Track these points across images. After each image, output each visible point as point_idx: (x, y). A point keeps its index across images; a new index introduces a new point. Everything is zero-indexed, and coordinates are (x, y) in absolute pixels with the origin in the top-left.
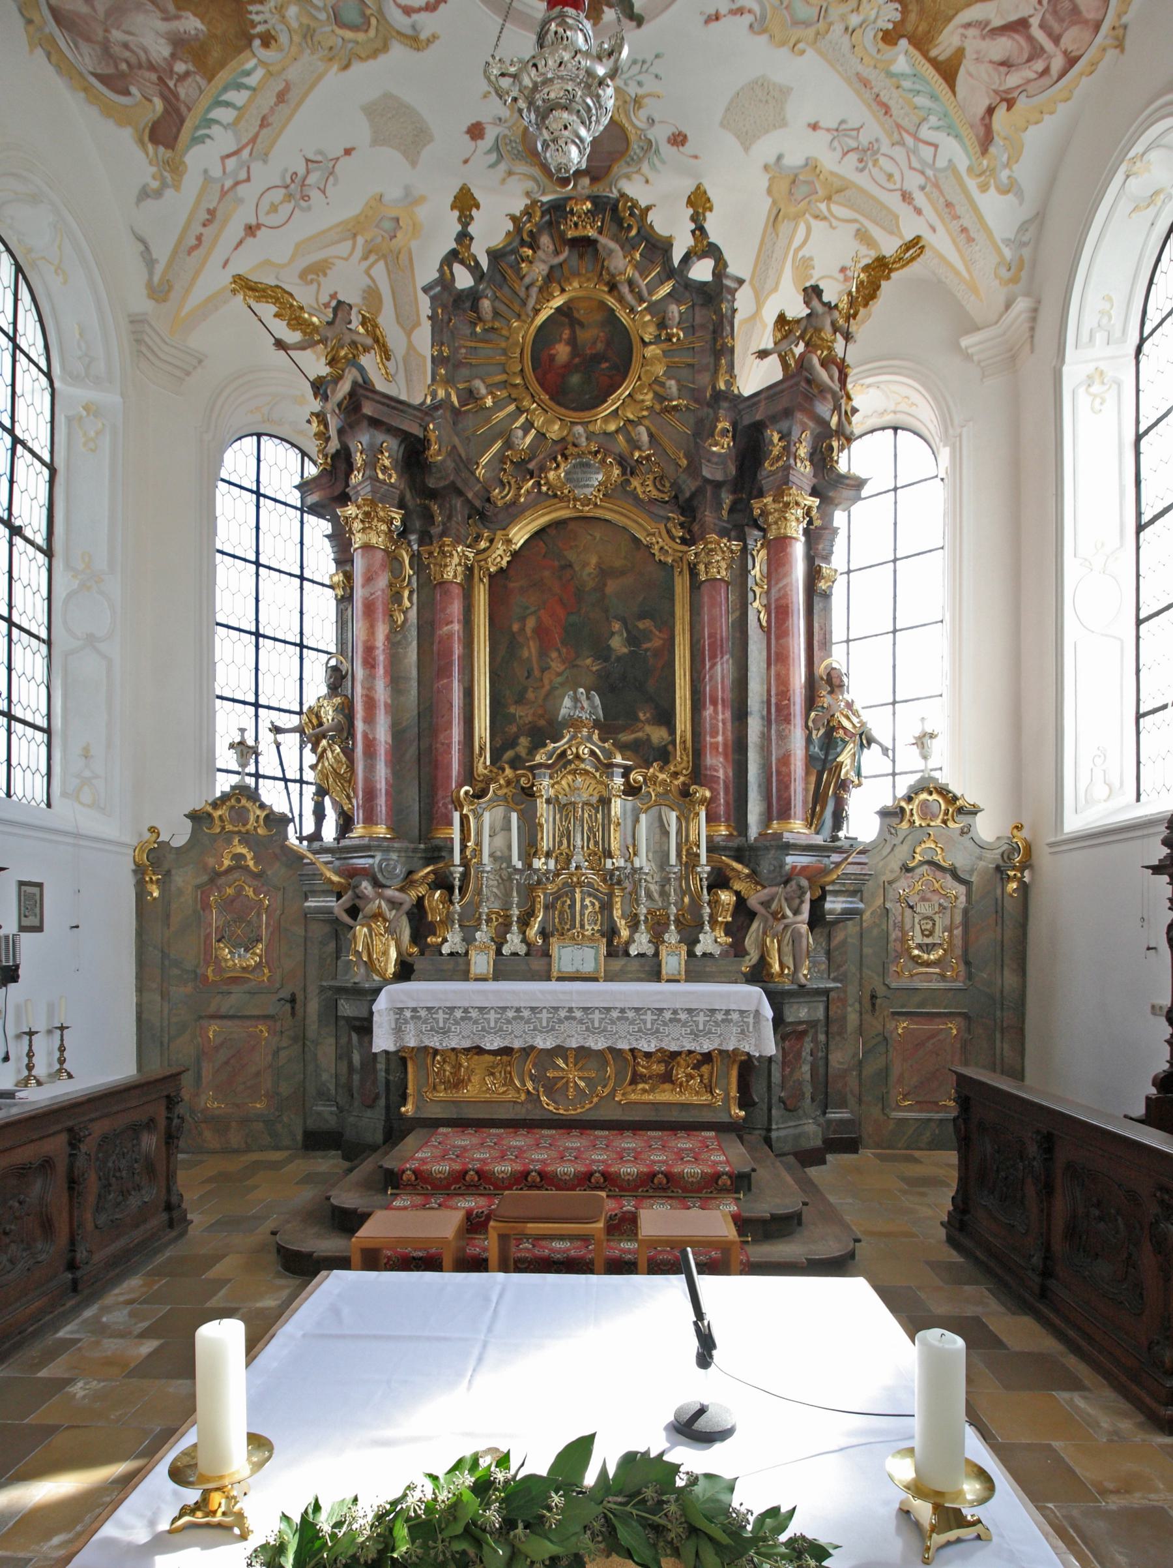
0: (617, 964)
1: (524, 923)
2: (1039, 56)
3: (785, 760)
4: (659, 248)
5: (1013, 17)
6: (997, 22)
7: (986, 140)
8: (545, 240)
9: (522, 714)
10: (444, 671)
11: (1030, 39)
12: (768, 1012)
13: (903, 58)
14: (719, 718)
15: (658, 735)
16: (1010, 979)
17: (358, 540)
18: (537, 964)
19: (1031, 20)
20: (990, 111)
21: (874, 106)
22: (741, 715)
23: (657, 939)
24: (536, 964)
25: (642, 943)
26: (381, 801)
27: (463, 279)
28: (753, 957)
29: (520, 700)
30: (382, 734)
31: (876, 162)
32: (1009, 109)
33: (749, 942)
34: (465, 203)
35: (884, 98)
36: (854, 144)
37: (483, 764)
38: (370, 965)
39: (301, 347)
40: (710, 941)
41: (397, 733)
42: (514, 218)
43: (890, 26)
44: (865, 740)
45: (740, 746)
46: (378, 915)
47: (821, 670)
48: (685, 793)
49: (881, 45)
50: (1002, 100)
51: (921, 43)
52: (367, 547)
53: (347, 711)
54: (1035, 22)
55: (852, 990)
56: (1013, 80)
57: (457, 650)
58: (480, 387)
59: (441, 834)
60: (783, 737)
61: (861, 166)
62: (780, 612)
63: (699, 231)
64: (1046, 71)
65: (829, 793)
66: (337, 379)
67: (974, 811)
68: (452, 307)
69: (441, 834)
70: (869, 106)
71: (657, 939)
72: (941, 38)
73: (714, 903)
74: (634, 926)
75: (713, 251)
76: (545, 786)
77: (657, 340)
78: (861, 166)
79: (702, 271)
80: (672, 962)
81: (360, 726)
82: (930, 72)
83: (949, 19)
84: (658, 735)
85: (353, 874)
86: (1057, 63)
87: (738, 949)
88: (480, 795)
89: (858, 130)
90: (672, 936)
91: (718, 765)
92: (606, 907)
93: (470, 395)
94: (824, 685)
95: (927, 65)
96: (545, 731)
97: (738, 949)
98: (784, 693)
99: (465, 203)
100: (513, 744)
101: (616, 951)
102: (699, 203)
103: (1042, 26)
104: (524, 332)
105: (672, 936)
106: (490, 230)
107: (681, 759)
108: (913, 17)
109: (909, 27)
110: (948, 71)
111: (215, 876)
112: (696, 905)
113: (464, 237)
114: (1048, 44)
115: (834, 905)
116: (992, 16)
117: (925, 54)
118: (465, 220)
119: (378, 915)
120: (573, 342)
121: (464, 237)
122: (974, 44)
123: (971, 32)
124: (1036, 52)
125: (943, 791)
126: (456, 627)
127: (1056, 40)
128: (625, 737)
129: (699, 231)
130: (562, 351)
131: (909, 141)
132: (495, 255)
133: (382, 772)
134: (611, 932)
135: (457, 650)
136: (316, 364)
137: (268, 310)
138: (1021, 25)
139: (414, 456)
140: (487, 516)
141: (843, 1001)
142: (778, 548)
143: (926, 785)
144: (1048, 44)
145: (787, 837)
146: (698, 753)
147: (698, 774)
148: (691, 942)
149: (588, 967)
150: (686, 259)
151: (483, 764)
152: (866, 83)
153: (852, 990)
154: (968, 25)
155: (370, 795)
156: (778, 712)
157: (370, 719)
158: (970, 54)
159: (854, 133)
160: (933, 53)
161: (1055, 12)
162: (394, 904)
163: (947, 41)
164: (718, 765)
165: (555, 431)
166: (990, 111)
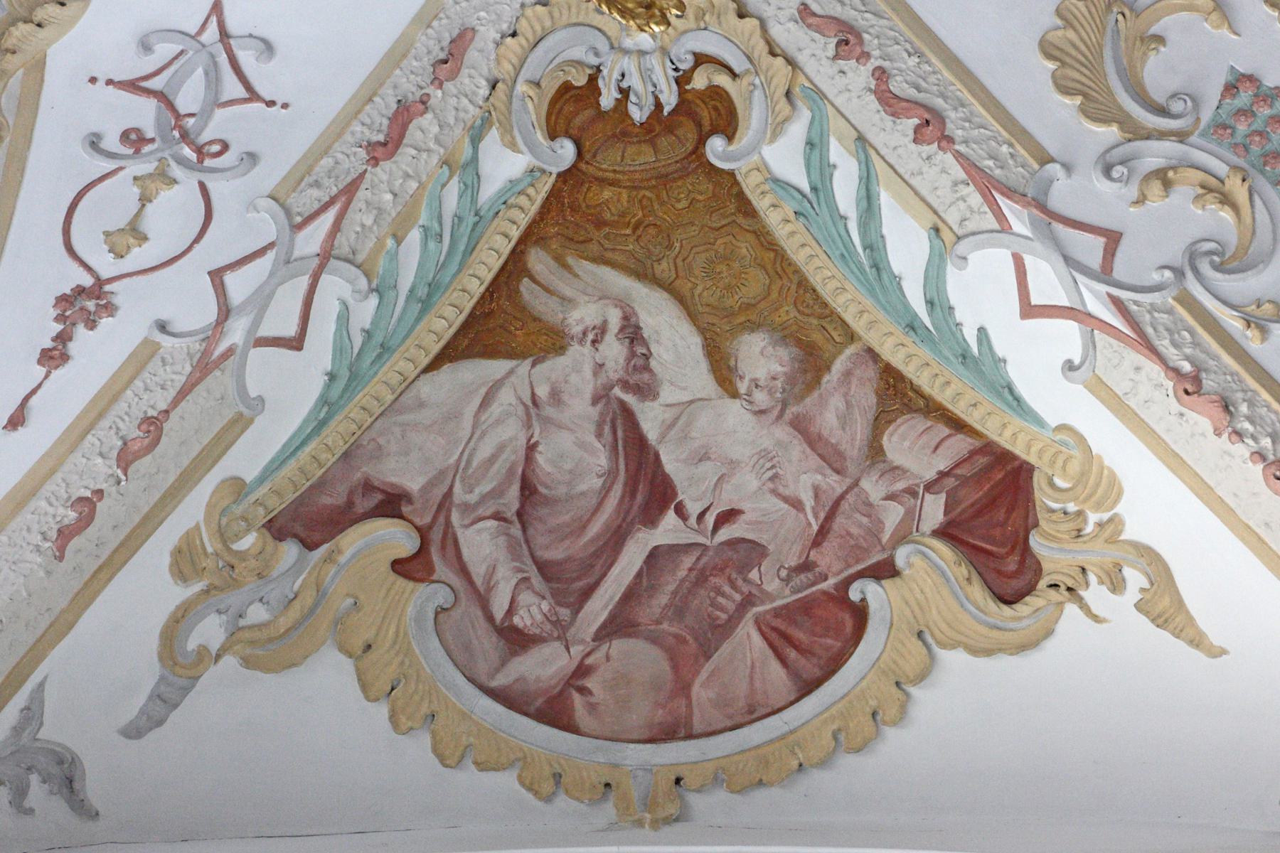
2: (559, 598)
5: (671, 463)
6: (651, 419)
7: (310, 521)
11: (615, 540)
13: (515, 164)
19: (670, 517)
20: (391, 504)
21: (386, 103)
31: (163, 177)
32: (399, 566)
35: (424, 128)
36: (189, 98)
43: (607, 100)
49: (551, 88)
50: (424, 533)
51: (566, 216)
54: (668, 530)
56: (481, 544)
61: (112, 142)
64: (516, 640)
70: (367, 96)
72: (585, 268)
78: (112, 142)
82: (489, 262)
83: (643, 274)
86: (543, 666)
89: (253, 96)
95: (506, 248)
103: (654, 556)
108: (642, 158)
109: (608, 160)
110: (496, 325)
114: (599, 608)
116: (668, 394)
117: (530, 237)
122: (576, 373)
123: (614, 351)
124: (568, 583)
127: (619, 624)
131: (311, 240)
138: (649, 489)
144: (599, 608)
152: (450, 61)
154: (633, 334)
158: (555, 366)
159: (233, 88)
160: (538, 261)
161: (701, 578)
163: (586, 295)
166: (391, 504)
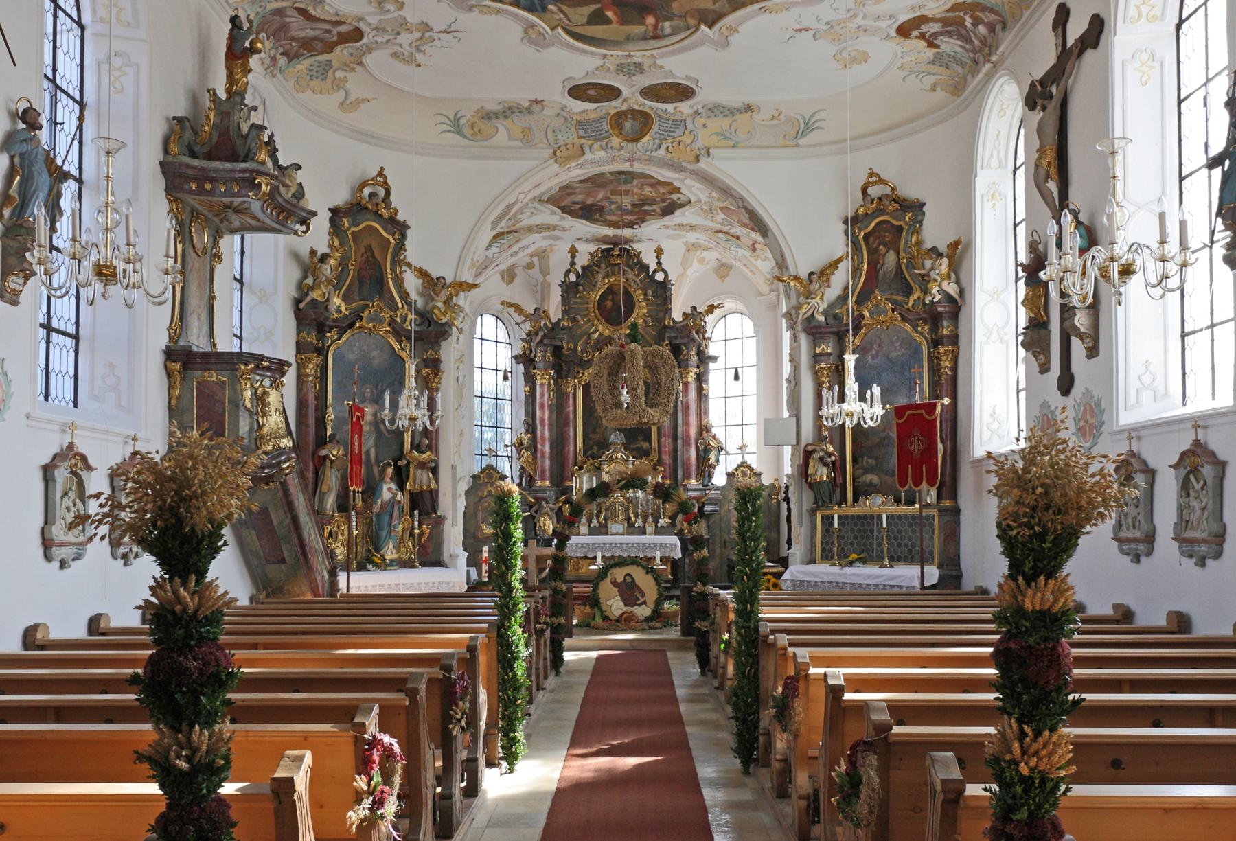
0: (631, 530)
1: (598, 516)
3: (689, 459)
4: (645, 268)
8: (603, 265)
9: (594, 437)
10: (566, 424)
12: (679, 544)
14: (667, 443)
15: (645, 445)
16: (774, 535)
17: (538, 382)
18: (603, 530)
22: (675, 438)
23: (645, 521)
24: (602, 530)
25: (639, 523)
26: (547, 473)
27: (573, 278)
28: (679, 527)
29: (594, 431)
30: (547, 449)
33: (677, 522)
34: (573, 252)
37: (580, 457)
38: (544, 531)
39: (523, 322)
40: (663, 522)
41: (551, 448)
42: (591, 255)
44: (720, 449)
45: (675, 450)
46: (547, 513)
47: (704, 423)
48: (655, 468)
52: (542, 385)
53: (534, 439)
55: (718, 540)
57: (571, 416)
58: (578, 317)
59: (568, 483)
60: (688, 451)
62: (686, 408)
63: (659, 263)
65: (705, 469)
66: (537, 334)
67: (760, 474)
68: (569, 289)
69: (568, 483)
71: (645, 521)
73: (664, 508)
74: (637, 517)
75: (663, 270)
76: (605, 467)
77: (644, 300)
79: (660, 277)
80: (649, 529)
81: (539, 446)
84: (645, 445)
85: (538, 500)
87: (673, 525)
88: (581, 468)
90: (650, 520)
91: (667, 459)
92: (627, 510)
93: (574, 320)
94: (704, 429)
96: (604, 445)
97: (673, 525)
98: (688, 436)
99: (573, 252)
100: (591, 448)
101: (630, 525)
102: (659, 252)
104: (596, 296)
105: (650, 520)
106: (582, 260)
107: (654, 456)
111: (482, 498)
112: (659, 509)
113: (573, 264)
115: (708, 508)
118: (573, 256)
119: (547, 513)
120: (612, 300)
121: (573, 264)
125: (749, 467)
126: (571, 408)
128: (633, 446)
129: (659, 263)
130: (609, 304)
132: (583, 268)
133: (547, 462)
134: (629, 519)
135: (571, 416)
136: (528, 326)
137: (511, 310)
139: (557, 351)
140: (584, 364)
141: (714, 544)
142: (686, 385)
143: (743, 464)
145: (689, 486)
146: (660, 452)
147: (660, 462)
148: (656, 521)
149: (621, 531)
150: (655, 272)
151: (580, 457)
153: (718, 540)
155: (543, 471)
156: (687, 443)
157: (543, 445)
162: (552, 509)
164: (667, 459)
165: (607, 333)
